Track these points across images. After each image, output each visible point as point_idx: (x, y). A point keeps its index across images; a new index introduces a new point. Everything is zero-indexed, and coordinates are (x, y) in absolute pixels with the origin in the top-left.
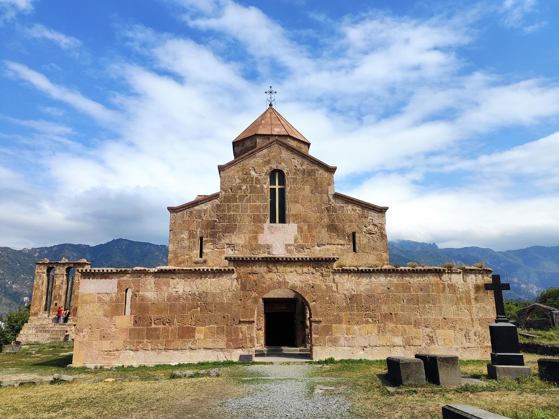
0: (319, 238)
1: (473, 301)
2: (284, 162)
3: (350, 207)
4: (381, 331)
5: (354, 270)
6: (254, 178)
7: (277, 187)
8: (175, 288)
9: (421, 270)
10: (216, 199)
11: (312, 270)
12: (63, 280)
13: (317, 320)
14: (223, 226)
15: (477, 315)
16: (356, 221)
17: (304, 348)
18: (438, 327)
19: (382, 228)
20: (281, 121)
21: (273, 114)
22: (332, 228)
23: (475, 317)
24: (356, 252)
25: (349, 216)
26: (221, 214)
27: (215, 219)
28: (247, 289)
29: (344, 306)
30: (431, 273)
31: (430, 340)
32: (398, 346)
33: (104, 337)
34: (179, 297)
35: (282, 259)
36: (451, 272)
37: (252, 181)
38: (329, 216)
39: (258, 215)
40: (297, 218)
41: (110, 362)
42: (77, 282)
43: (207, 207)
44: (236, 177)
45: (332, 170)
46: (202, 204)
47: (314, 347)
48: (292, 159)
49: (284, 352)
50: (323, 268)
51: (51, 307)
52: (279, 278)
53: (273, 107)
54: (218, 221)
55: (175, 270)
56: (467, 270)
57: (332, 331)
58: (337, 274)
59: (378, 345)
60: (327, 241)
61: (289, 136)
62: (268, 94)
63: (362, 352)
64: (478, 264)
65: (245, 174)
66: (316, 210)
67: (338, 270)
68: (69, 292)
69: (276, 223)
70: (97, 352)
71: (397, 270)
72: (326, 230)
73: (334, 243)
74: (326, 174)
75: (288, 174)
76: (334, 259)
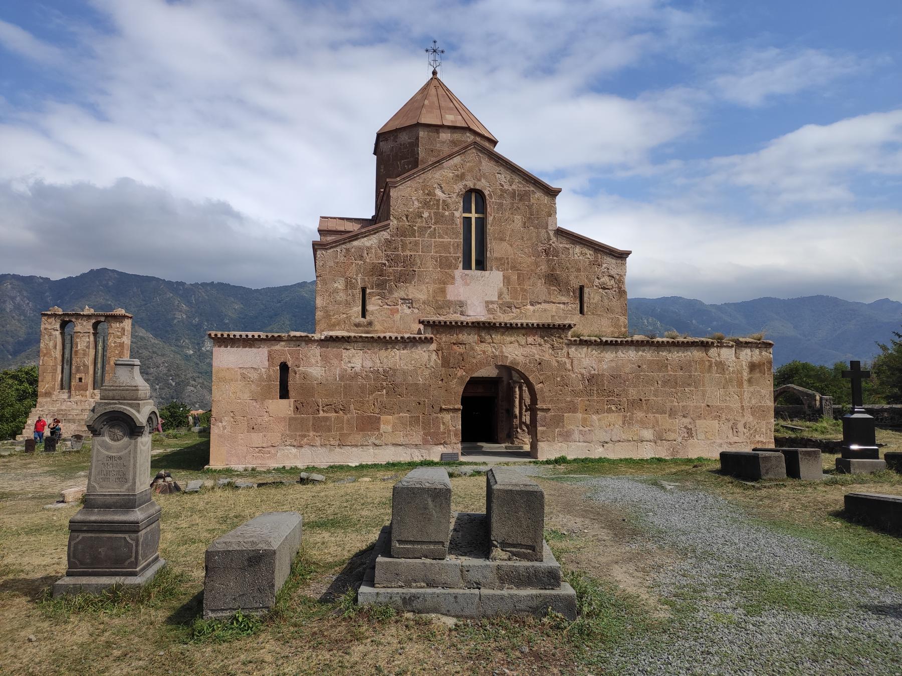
0: (533, 293)
1: (745, 384)
2: (486, 178)
3: (578, 249)
4: (627, 422)
5: (595, 341)
6: (441, 201)
7: (473, 215)
8: (350, 362)
9: (683, 342)
10: (384, 230)
11: (539, 340)
12: (89, 342)
13: (545, 408)
14: (395, 272)
15: (749, 402)
16: (585, 269)
17: (510, 445)
18: (699, 417)
19: (620, 281)
20: (454, 102)
21: (440, 90)
22: (552, 279)
23: (746, 404)
24: (584, 315)
25: (576, 262)
26: (392, 254)
27: (384, 262)
28: (451, 365)
29: (580, 389)
30: (695, 346)
31: (688, 433)
32: (647, 441)
33: (253, 429)
34: (356, 374)
35: (500, 324)
36: (721, 345)
37: (438, 205)
39: (447, 257)
40: (502, 263)
41: (264, 462)
42: (112, 344)
43: (371, 242)
44: (414, 198)
46: (363, 237)
47: (539, 443)
48: (496, 174)
49: (484, 449)
50: (554, 338)
51: (73, 383)
52: (494, 351)
53: (438, 76)
54: (387, 264)
55: (349, 337)
56: (741, 342)
57: (563, 422)
58: (572, 346)
59: (622, 440)
60: (544, 298)
62: (431, 53)
63: (601, 449)
64: (756, 335)
65: (428, 194)
66: (529, 252)
67: (575, 341)
68: (99, 360)
70: (245, 449)
71: (653, 342)
72: (543, 281)
73: (554, 301)
74: (546, 199)
76: (570, 327)
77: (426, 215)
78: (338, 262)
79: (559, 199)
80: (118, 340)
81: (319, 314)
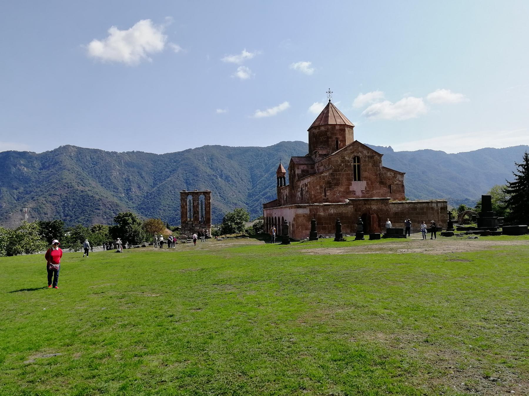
0: (376, 187)
2: (360, 152)
3: (389, 173)
7: (356, 164)
21: (333, 108)
22: (382, 183)
23: (440, 219)
37: (346, 162)
38: (380, 177)
40: (366, 178)
45: (380, 156)
53: (331, 102)
61: (345, 125)
69: (356, 181)
75: (362, 158)
76: (389, 199)
77: (343, 165)
78: (317, 181)
79: (383, 158)
80: (209, 201)
81: (313, 196)
